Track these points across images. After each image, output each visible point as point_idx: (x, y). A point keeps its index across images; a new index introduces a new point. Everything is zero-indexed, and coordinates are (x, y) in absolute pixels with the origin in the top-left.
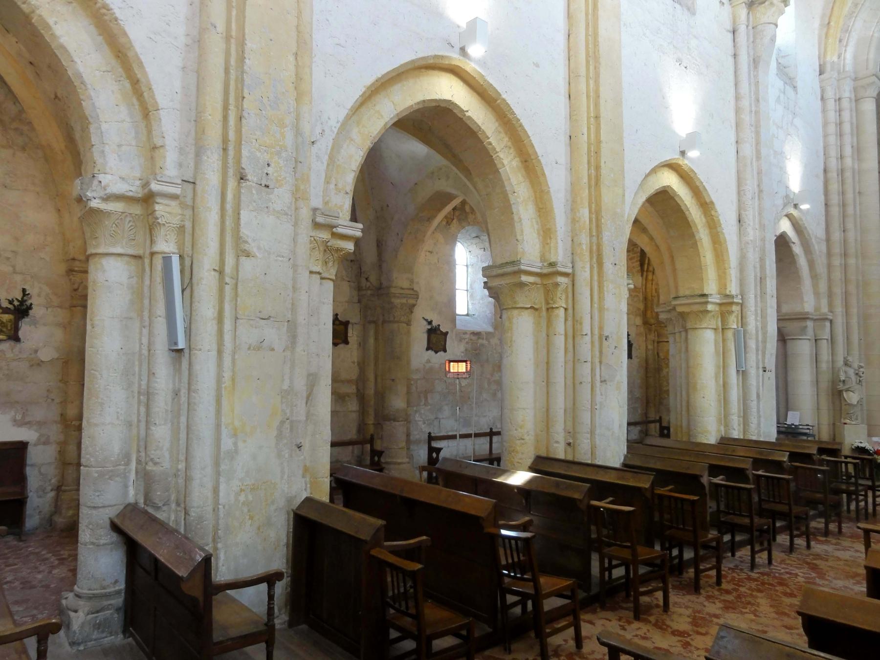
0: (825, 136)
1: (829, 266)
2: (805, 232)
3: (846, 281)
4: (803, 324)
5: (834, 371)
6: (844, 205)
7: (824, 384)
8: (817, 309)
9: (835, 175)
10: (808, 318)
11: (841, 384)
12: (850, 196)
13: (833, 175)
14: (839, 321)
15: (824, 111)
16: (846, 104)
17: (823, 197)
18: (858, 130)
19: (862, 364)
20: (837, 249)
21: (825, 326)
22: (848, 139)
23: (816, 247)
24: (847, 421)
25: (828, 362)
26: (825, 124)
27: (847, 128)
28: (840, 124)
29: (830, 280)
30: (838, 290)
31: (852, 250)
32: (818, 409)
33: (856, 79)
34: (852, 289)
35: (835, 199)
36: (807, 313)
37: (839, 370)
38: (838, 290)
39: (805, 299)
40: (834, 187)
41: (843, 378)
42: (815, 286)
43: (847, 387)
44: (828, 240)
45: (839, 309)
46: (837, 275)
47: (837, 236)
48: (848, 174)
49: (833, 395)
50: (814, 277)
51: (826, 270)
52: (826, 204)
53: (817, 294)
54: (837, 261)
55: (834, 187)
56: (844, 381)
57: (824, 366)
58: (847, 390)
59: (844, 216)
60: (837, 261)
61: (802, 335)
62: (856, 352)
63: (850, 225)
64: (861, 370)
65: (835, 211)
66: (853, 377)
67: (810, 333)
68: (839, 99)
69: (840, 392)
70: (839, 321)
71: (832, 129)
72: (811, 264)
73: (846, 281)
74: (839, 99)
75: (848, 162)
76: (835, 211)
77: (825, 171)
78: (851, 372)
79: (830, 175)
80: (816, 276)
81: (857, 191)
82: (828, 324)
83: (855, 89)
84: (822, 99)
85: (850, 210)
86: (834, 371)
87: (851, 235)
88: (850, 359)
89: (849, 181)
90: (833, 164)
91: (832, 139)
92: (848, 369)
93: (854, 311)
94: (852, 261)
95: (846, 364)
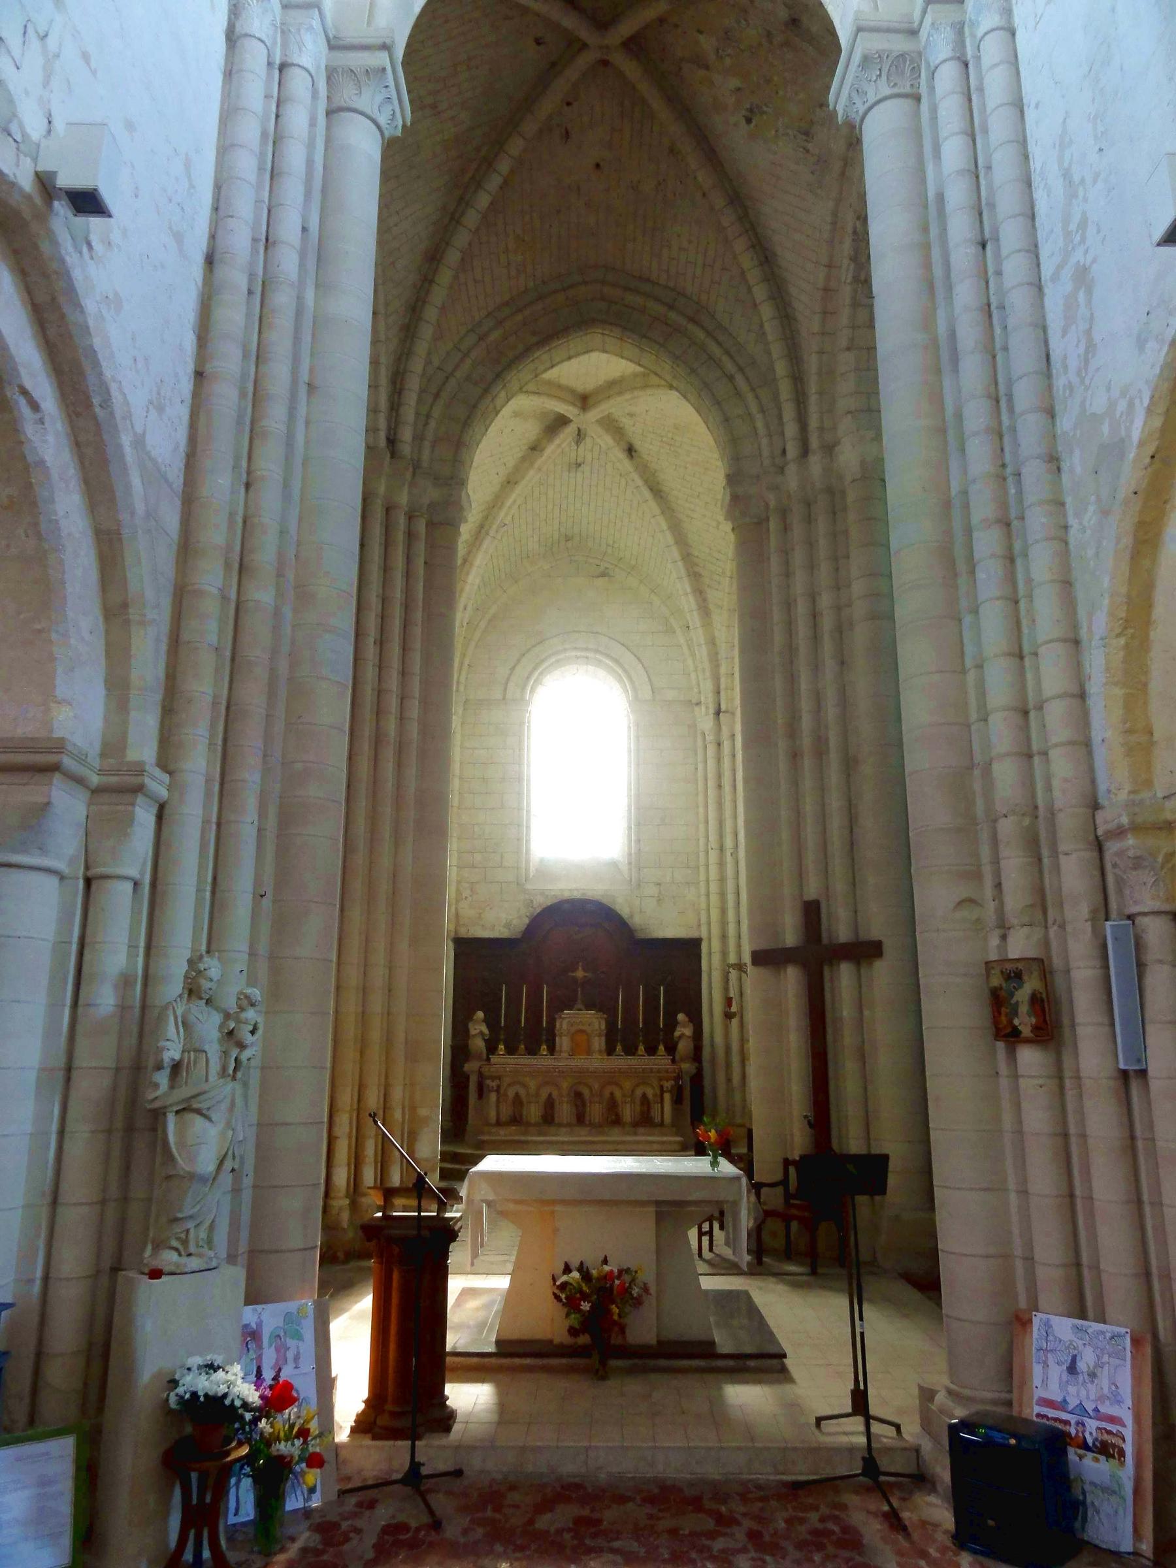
0: (225, 149)
1: (182, 596)
2: (92, 380)
3: (236, 663)
4: (26, 793)
5: (143, 1019)
6: (257, 396)
7: (91, 1086)
8: (114, 746)
9: (242, 281)
10: (55, 768)
11: (162, 1079)
12: (279, 373)
13: (235, 277)
14: (193, 813)
15: (230, 73)
16: (299, 84)
17: (189, 341)
18: (326, 190)
19: (256, 993)
20: (216, 534)
21: (130, 820)
22: (293, 190)
23: (136, 480)
24: (168, 1258)
25: (126, 982)
26: (229, 113)
27: (295, 157)
28: (277, 139)
29: (175, 642)
30: (204, 687)
31: (266, 554)
32: (55, 1202)
33: (335, 45)
34: (254, 696)
35: (230, 361)
36: (59, 746)
37: (161, 1019)
38: (204, 687)
39: (61, 691)
40: (233, 315)
41: (173, 1053)
42: (117, 656)
43: (183, 1092)
44: (189, 499)
45: (198, 763)
46: (209, 629)
47: (220, 484)
48: (283, 299)
49: (130, 1129)
50: (116, 611)
51: (166, 602)
52: (199, 375)
53: (118, 687)
54: (211, 577)
55: (233, 315)
56: (176, 1067)
57: (104, 999)
58: (186, 1109)
59: (255, 433)
60: (211, 577)
61: (24, 849)
62: (238, 939)
63: (270, 464)
64: (250, 1014)
65: (226, 398)
66: (213, 1050)
67: (64, 845)
68: (283, 67)
69: (157, 1116)
70: (193, 813)
71: (250, 131)
72: (109, 546)
73: (236, 663)
74: (283, 67)
75: (288, 261)
76: (226, 398)
77: (210, 260)
78: (209, 1026)
79: (221, 272)
80: (125, 605)
81: (305, 377)
82: (145, 817)
83: (331, 74)
84: (232, 38)
85: (275, 417)
86: (143, 1019)
87: (269, 501)
88: (213, 967)
89: (283, 322)
90: (240, 240)
91: (246, 165)
92: (198, 1009)
93: (250, 777)
94: (262, 594)
95: (192, 991)
